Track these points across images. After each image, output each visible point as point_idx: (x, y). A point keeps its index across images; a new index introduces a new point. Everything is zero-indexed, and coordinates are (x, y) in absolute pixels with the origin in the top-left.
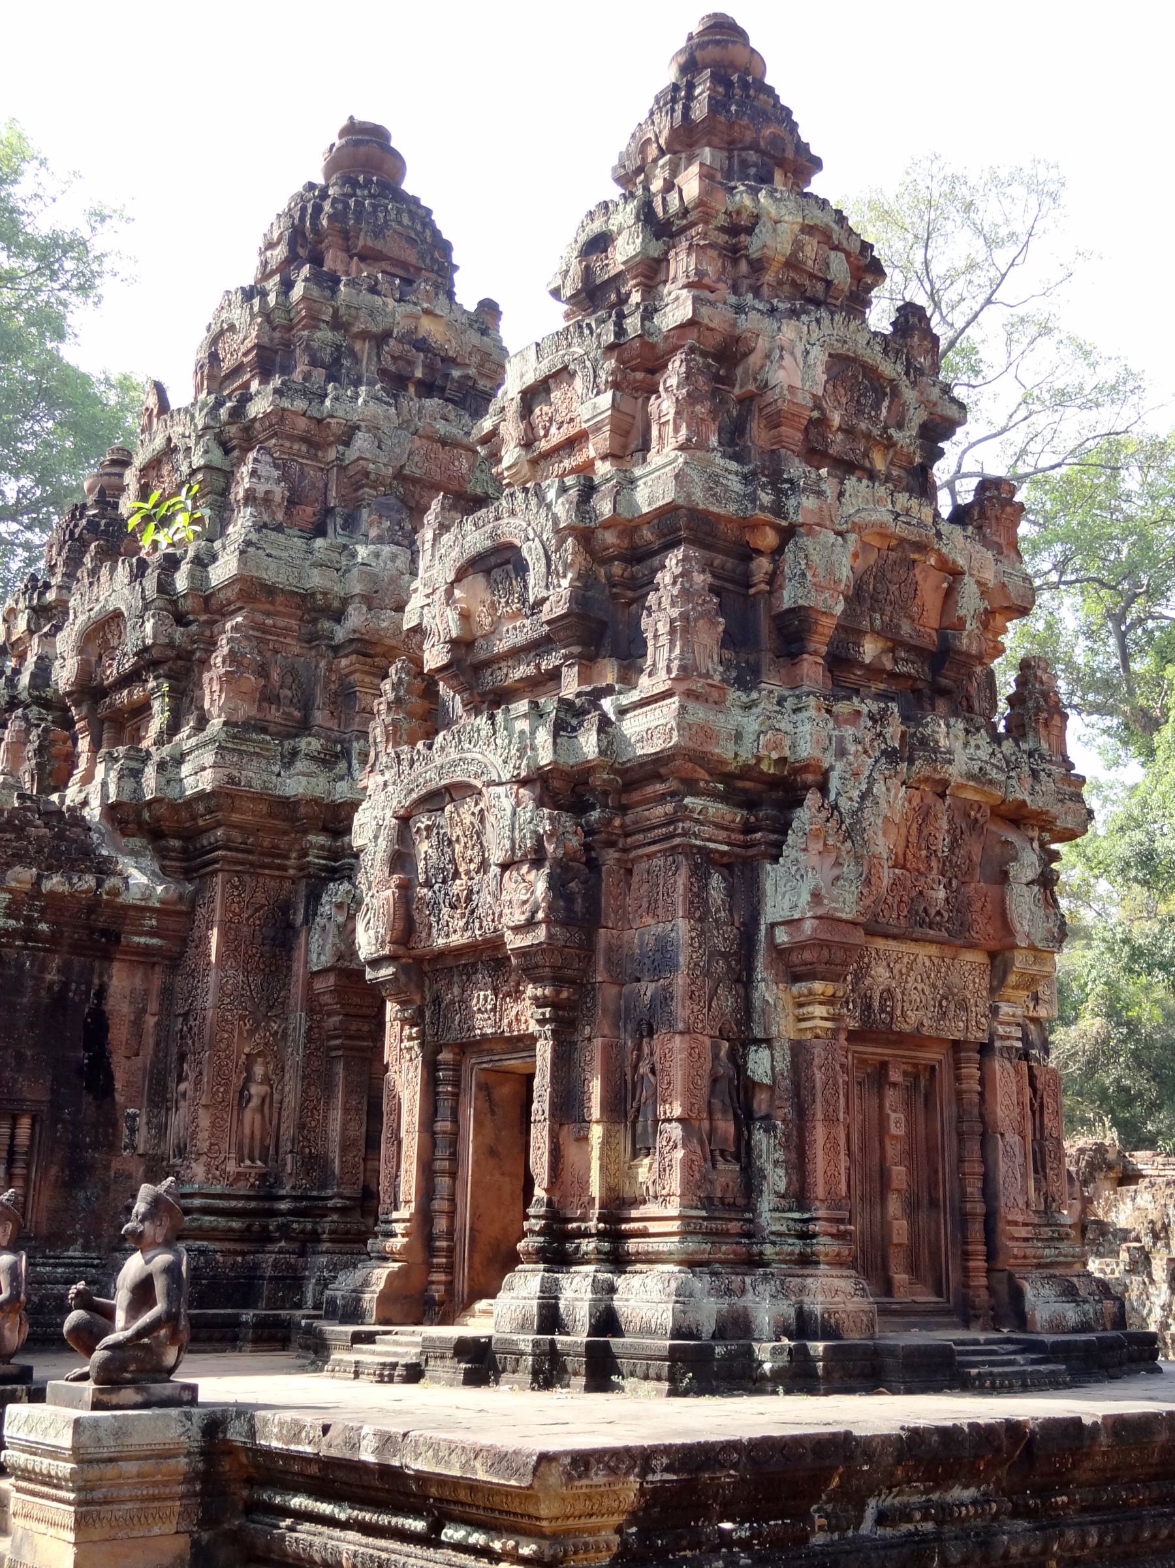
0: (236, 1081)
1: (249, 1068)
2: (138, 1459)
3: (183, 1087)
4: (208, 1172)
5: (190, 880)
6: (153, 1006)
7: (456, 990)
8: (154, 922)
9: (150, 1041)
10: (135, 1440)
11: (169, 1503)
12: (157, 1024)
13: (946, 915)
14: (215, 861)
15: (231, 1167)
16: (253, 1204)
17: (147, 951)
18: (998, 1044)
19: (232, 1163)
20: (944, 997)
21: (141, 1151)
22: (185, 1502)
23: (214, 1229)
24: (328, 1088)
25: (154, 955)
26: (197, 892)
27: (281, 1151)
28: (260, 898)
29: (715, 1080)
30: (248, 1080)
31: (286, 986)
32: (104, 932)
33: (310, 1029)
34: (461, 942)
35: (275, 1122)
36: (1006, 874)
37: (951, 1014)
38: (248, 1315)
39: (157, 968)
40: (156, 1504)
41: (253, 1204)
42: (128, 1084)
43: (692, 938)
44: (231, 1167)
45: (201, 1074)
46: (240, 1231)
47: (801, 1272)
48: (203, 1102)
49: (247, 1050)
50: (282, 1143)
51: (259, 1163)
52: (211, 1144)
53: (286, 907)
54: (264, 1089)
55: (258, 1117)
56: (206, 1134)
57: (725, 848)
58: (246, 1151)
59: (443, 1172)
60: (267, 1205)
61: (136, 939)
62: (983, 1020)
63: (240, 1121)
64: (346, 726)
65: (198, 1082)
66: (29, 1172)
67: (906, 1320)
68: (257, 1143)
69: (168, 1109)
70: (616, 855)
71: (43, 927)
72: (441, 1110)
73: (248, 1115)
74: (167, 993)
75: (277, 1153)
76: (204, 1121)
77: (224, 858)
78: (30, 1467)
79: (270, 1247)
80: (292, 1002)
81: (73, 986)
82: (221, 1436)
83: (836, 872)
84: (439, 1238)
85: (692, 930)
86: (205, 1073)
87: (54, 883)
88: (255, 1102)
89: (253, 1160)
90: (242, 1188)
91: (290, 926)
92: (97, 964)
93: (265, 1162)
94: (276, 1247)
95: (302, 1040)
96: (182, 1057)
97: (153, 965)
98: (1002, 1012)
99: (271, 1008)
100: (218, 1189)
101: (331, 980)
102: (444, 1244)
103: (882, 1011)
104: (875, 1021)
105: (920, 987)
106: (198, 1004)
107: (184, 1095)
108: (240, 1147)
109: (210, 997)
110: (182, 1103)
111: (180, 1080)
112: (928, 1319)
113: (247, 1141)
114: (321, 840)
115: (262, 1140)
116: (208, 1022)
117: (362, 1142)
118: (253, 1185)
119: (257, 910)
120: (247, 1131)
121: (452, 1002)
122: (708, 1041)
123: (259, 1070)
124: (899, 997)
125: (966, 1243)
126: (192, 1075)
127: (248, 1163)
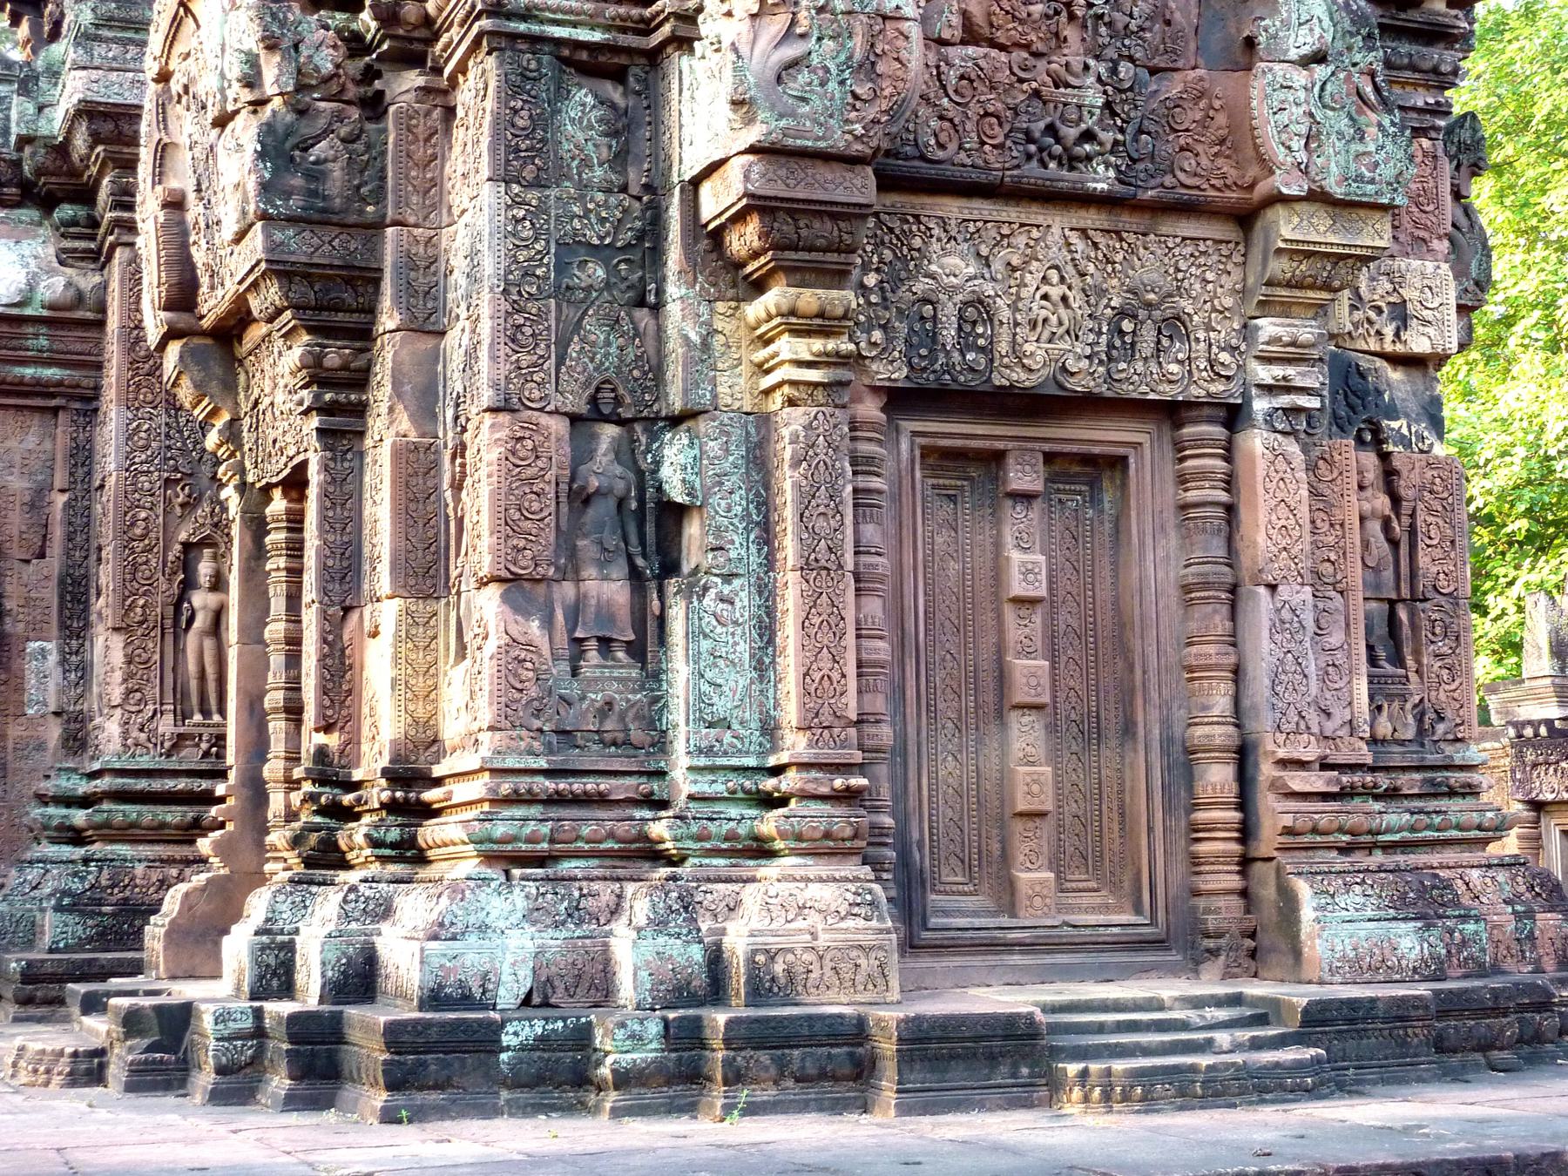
0: (166, 588)
4: (125, 735)
6: (60, 479)
8: (43, 342)
9: (58, 532)
12: (68, 505)
13: (1103, 136)
15: (166, 726)
17: (40, 389)
18: (1260, 405)
20: (1122, 313)
23: (134, 825)
25: (53, 396)
29: (580, 499)
30: (189, 584)
36: (1250, 43)
37: (1146, 347)
39: (61, 414)
42: (28, 602)
43: (518, 221)
44: (166, 726)
47: (735, 872)
49: (183, 536)
52: (129, 692)
56: (118, 676)
57: (597, 36)
58: (195, 700)
62: (1224, 357)
63: (179, 651)
67: (1049, 959)
70: (421, 81)
83: (791, 51)
85: (516, 203)
89: (206, 713)
97: (55, 411)
98: (1263, 336)
100: (145, 762)
103: (966, 341)
104: (949, 368)
105: (1055, 292)
108: (181, 695)
112: (1106, 958)
118: (206, 754)
120: (192, 667)
122: (558, 426)
123: (205, 569)
124: (1005, 315)
125: (1195, 807)
127: (198, 718)
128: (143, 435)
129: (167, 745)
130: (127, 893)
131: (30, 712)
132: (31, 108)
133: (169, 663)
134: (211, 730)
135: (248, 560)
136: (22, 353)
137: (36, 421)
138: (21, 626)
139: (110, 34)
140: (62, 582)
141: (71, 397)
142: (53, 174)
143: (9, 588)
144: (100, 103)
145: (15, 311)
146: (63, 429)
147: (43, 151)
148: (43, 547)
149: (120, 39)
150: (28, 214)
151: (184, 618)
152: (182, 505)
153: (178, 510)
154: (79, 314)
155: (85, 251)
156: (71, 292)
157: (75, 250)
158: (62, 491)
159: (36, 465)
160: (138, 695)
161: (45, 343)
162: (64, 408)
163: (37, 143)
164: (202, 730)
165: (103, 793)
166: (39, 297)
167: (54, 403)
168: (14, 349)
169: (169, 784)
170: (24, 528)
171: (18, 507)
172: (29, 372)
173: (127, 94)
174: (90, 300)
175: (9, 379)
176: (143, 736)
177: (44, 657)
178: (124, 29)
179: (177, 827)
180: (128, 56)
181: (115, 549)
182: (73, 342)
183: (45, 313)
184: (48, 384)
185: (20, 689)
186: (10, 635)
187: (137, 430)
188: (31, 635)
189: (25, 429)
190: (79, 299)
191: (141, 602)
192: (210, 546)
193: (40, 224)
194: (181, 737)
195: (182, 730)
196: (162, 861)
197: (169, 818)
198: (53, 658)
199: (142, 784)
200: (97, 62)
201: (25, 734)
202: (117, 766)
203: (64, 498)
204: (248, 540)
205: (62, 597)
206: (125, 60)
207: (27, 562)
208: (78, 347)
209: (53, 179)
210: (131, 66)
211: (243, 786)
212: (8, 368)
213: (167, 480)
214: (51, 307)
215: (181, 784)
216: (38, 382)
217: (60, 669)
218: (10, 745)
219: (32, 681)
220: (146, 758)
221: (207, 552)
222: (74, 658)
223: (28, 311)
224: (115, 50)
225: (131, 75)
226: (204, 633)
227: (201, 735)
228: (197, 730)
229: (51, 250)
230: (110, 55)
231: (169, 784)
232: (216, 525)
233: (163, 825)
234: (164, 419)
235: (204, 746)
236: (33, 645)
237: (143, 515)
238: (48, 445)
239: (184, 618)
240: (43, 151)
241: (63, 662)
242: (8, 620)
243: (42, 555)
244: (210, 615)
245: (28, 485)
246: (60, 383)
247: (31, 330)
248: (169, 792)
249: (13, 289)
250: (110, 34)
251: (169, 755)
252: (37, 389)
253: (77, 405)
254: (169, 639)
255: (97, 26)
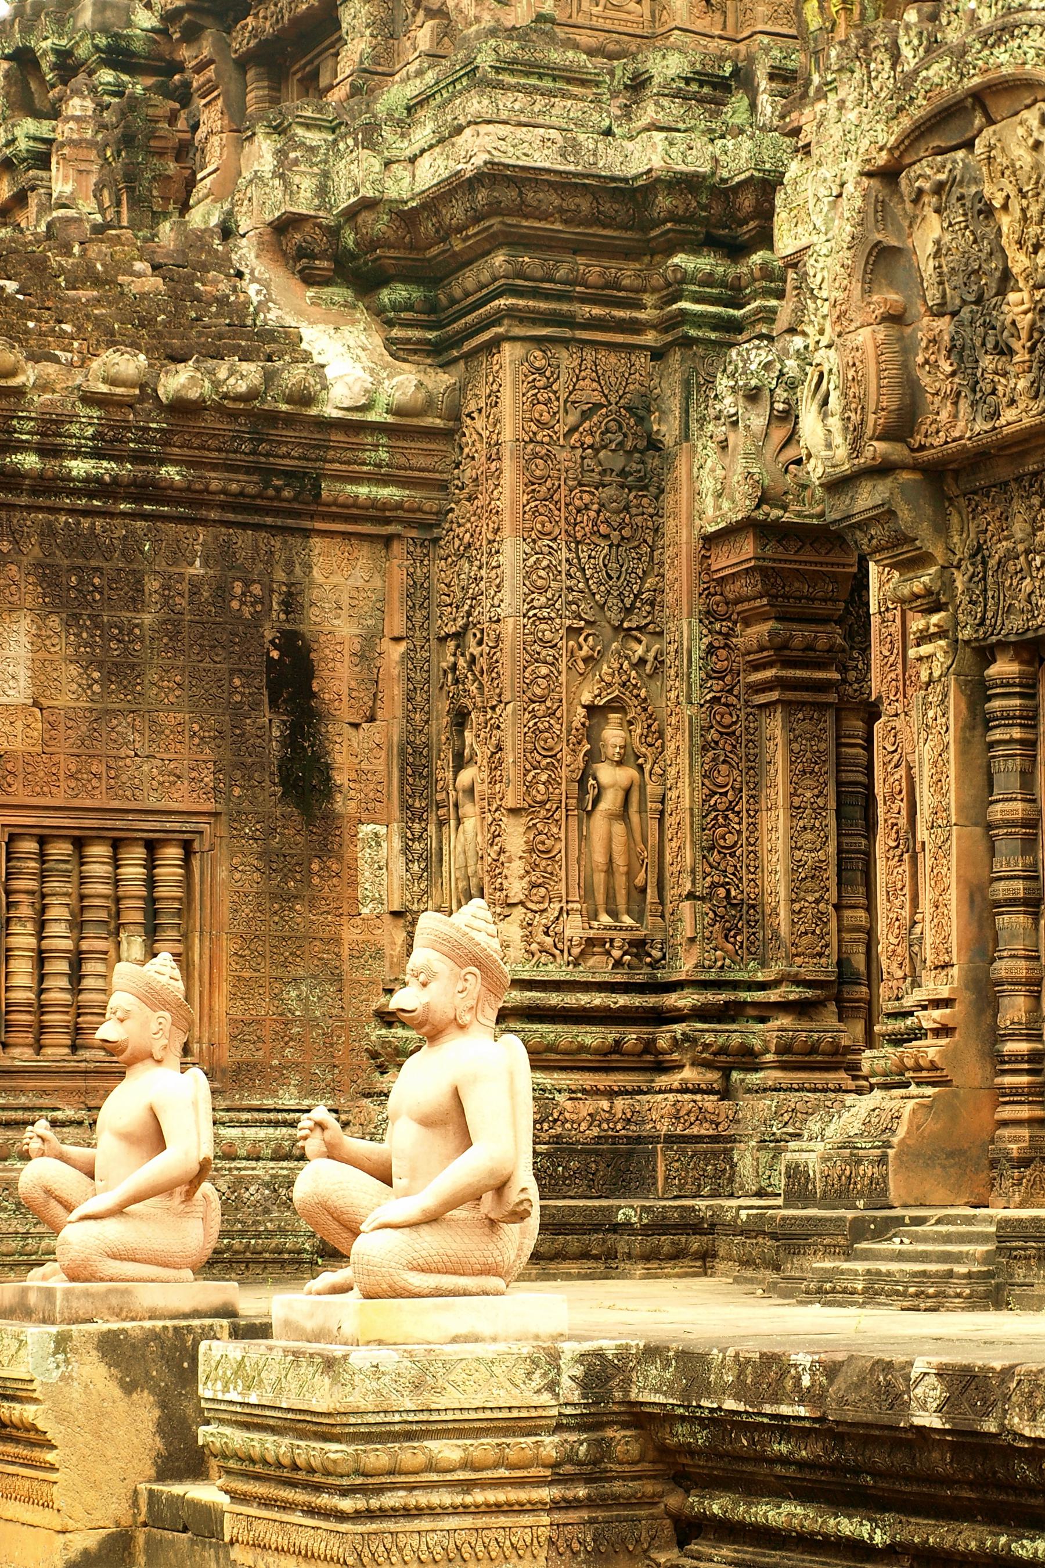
0: (570, 763)
1: (591, 733)
2: (461, 1433)
3: (466, 776)
4: (528, 939)
5: (444, 366)
6: (397, 624)
7: (1019, 528)
9: (395, 692)
10: (451, 1399)
11: (527, 1520)
12: (407, 657)
14: (494, 320)
16: (622, 1000)
19: (576, 920)
21: (396, 907)
22: (559, 1517)
24: (755, 767)
25: (387, 521)
26: (461, 389)
27: (670, 894)
28: (589, 393)
30: (593, 757)
31: (654, 565)
32: (289, 475)
33: (711, 650)
34: (1027, 422)
35: (653, 839)
38: (628, 1210)
39: (396, 547)
40: (503, 1520)
41: (622, 1000)
44: (574, 928)
45: (499, 748)
46: (604, 1052)
48: (510, 802)
49: (586, 698)
50: (669, 881)
51: (627, 920)
53: (642, 408)
54: (626, 774)
55: (619, 828)
56: (517, 867)
58: (600, 898)
59: (1012, 902)
60: (650, 1000)
61: (352, 489)
63: (584, 838)
64: (738, 26)
65: (495, 764)
66: (189, 949)
68: (621, 881)
69: (441, 823)
71: (171, 472)
72: (999, 779)
73: (599, 824)
74: (419, 596)
75: (662, 902)
76: (515, 837)
77: (511, 313)
78: (256, 1452)
79: (663, 1080)
80: (670, 598)
81: (238, 588)
82: (618, 1395)
84: (1012, 1036)
86: (508, 744)
87: (179, 381)
88: (610, 802)
89: (614, 914)
90: (599, 968)
91: (654, 445)
92: (277, 543)
93: (639, 918)
94: (673, 1079)
95: (696, 676)
96: (460, 719)
97: (388, 541)
99: (629, 611)
100: (555, 971)
101: (747, 549)
102: (1022, 1047)
106: (483, 612)
107: (470, 791)
108: (588, 892)
109: (506, 594)
110: (468, 809)
111: (460, 762)
113: (599, 878)
114: (703, 263)
115: (630, 875)
116: (506, 645)
117: (832, 872)
119: (585, 415)
120: (599, 857)
121: (1011, 555)
123: (613, 735)
126: (482, 753)
127: (605, 919)
128: (542, 573)
129: (576, 951)
130: (559, 1130)
131: (365, 911)
132: (377, 165)
133: (574, 854)
134: (624, 934)
135: (963, 729)
136: (356, 468)
137: (364, 554)
138: (353, 804)
139: (513, 81)
140: (402, 752)
141: (409, 524)
142: (391, 247)
143: (339, 758)
144: (507, 166)
145: (357, 416)
146: (399, 563)
147: (386, 218)
148: (373, 709)
149: (524, 86)
150: (340, 293)
151: (590, 797)
152: (586, 660)
153: (581, 664)
154: (429, 421)
155: (420, 341)
156: (421, 395)
157: (408, 341)
158: (397, 640)
159: (366, 607)
160: (542, 890)
161: (385, 456)
162: (399, 536)
163: (380, 208)
164: (614, 934)
165: (513, 1008)
166: (382, 400)
167: (391, 529)
168: (348, 463)
169: (584, 999)
170: (353, 684)
171: (347, 658)
172: (363, 491)
173: (536, 155)
174: (442, 403)
175: (341, 500)
176: (549, 941)
177: (378, 844)
178: (528, 74)
179: (597, 1051)
180: (536, 108)
181: (514, 711)
182: (418, 456)
183: (390, 419)
184: (385, 506)
185: (354, 884)
186: (341, 816)
187: (535, 567)
188: (364, 816)
189: (352, 562)
190: (429, 406)
191: (544, 777)
192: (615, 710)
193: (354, 307)
194: (590, 942)
195: (591, 933)
196: (584, 1091)
197: (588, 1040)
198: (397, 844)
199: (554, 999)
200: (504, 115)
201: (361, 937)
202: (526, 976)
203: (402, 647)
204: (963, 706)
205: (402, 770)
206: (532, 112)
207: (356, 726)
208: (422, 462)
209: (392, 253)
210: (540, 120)
211: (967, 988)
212: (338, 486)
213: (570, 629)
214: (397, 411)
215: (597, 999)
216: (373, 503)
217: (403, 859)
218: (346, 952)
219: (366, 873)
220: (551, 967)
221: (614, 717)
222: (416, 846)
223: (372, 417)
224: (522, 100)
225: (542, 130)
226: (612, 817)
227: (612, 940)
228: (608, 934)
229: (378, 340)
230: (517, 106)
231: (584, 999)
232: (624, 685)
233: (582, 1048)
234: (564, 554)
235: (616, 953)
236: (366, 830)
237: (544, 671)
238: (377, 582)
239: (590, 797)
240: (386, 218)
241: (406, 849)
242: (339, 797)
243: (372, 719)
244: (621, 795)
245: (357, 631)
246: (399, 506)
247: (369, 440)
248: (584, 1009)
249: (357, 388)
250: (513, 81)
251: (576, 964)
252: (372, 512)
253: (414, 533)
254: (574, 823)
255: (497, 70)
